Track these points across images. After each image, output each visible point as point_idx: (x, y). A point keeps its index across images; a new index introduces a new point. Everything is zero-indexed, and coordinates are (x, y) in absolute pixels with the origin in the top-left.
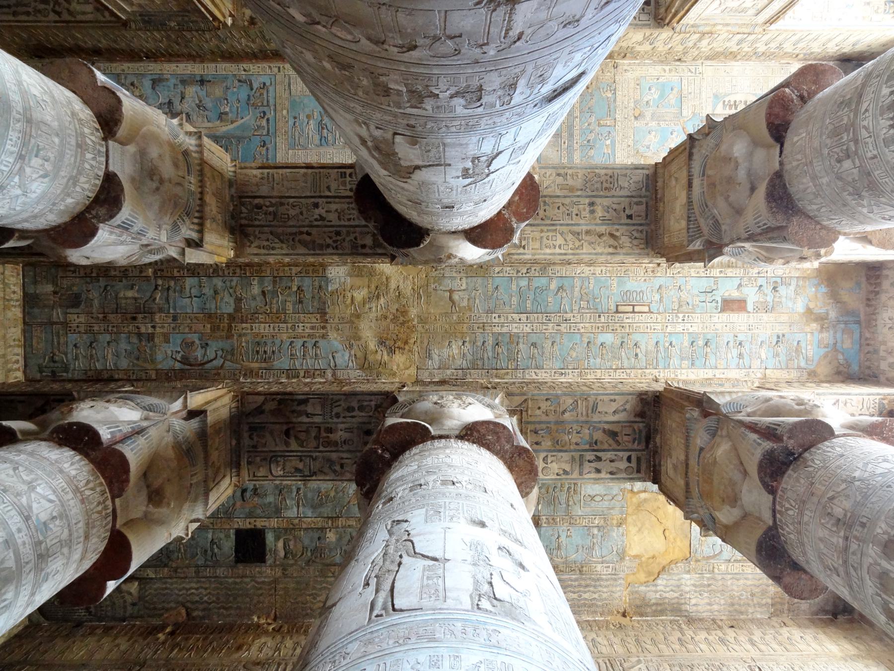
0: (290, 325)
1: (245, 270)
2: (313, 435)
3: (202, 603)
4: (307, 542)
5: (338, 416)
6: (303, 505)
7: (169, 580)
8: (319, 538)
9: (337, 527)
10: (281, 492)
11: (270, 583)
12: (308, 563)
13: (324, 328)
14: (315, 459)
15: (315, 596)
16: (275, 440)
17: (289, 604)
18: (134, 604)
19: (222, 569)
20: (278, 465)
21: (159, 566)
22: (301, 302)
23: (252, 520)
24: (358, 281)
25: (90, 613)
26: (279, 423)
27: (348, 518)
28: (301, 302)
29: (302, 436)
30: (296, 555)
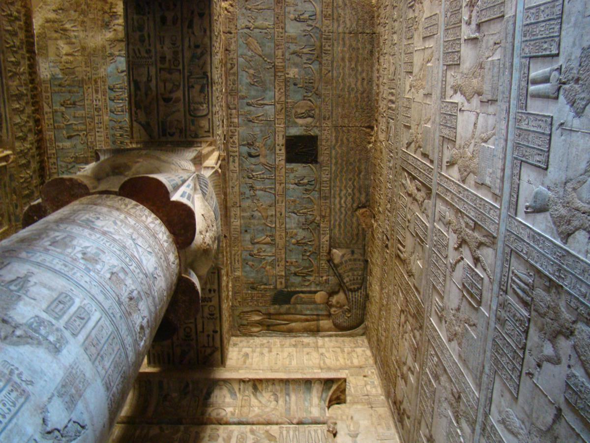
0: (96, 113)
1: (51, 154)
2: (167, 76)
3: (354, 194)
4: (299, 97)
5: (148, 51)
6: (263, 99)
7: (332, 222)
8: (295, 84)
9: (284, 67)
10: (250, 121)
11: (337, 132)
12: (318, 95)
13: (96, 82)
14: (191, 73)
15: (350, 90)
16: (174, 112)
17: (357, 114)
18: (353, 253)
19: (323, 176)
20: (198, 109)
21: (319, 231)
22: (74, 104)
23: (278, 148)
24: (52, 50)
25: (359, 289)
26: (158, 108)
27: (276, 57)
28: (74, 104)
29: (169, 86)
30: (310, 107)
